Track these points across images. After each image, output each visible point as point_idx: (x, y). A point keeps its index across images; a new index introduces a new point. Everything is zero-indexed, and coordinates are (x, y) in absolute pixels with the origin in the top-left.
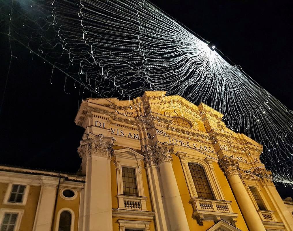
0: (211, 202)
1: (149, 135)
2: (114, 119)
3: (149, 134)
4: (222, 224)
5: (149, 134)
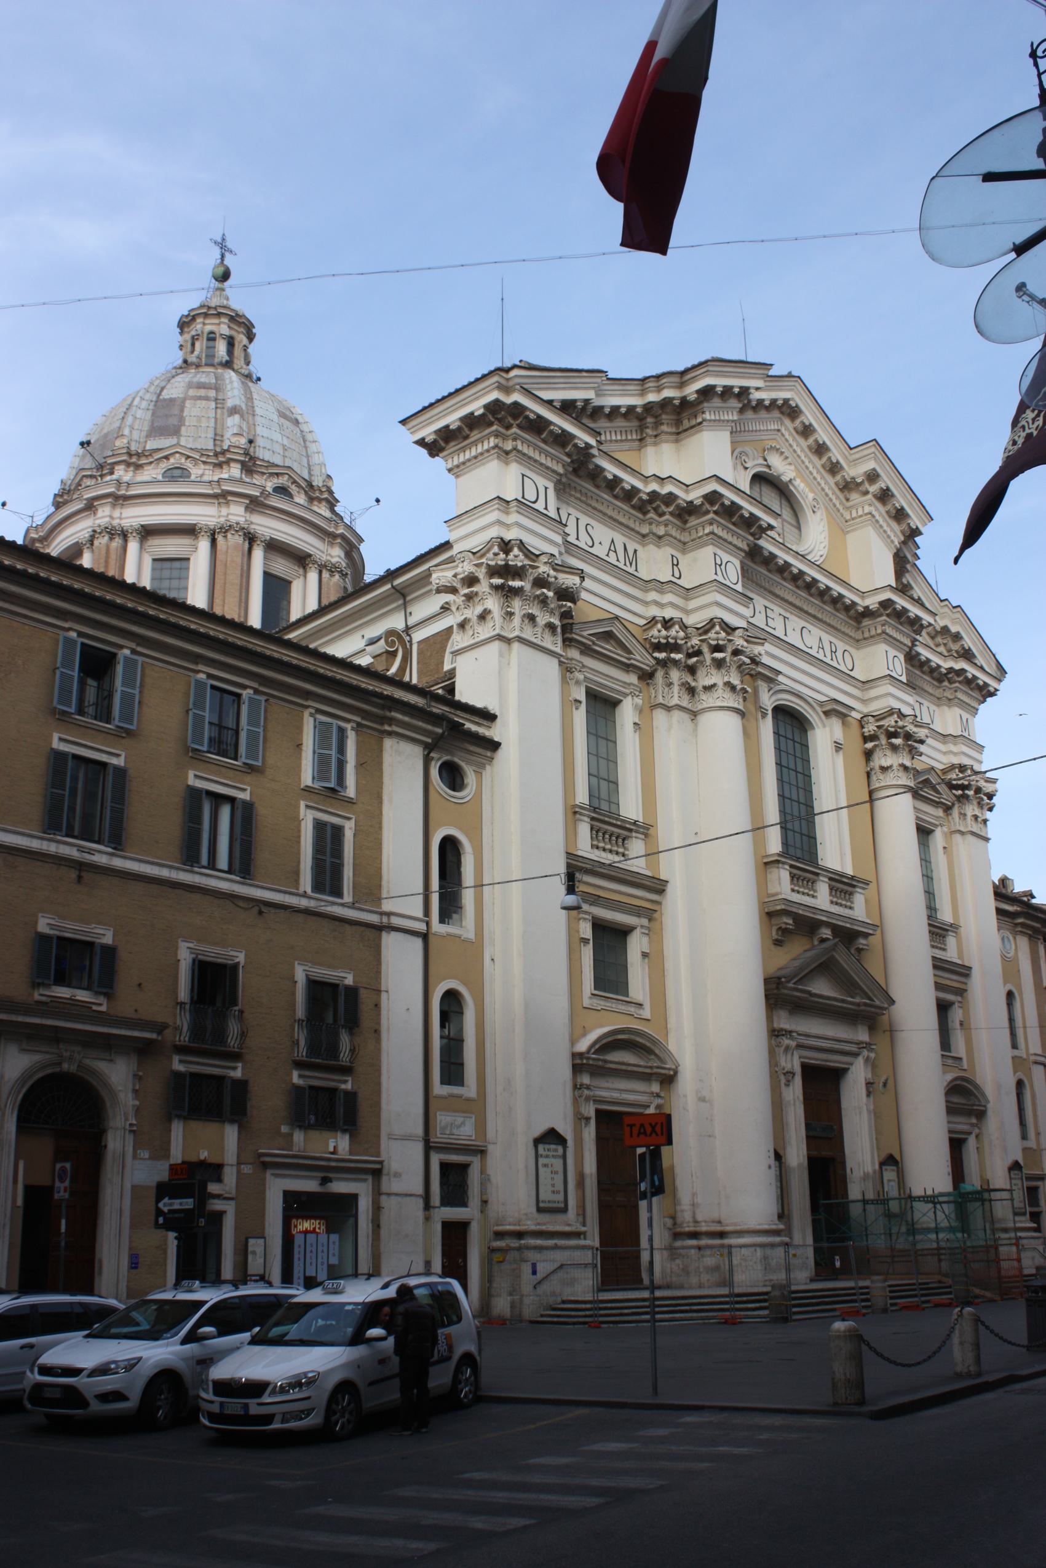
1: (677, 565)
3: (675, 563)
5: (675, 563)
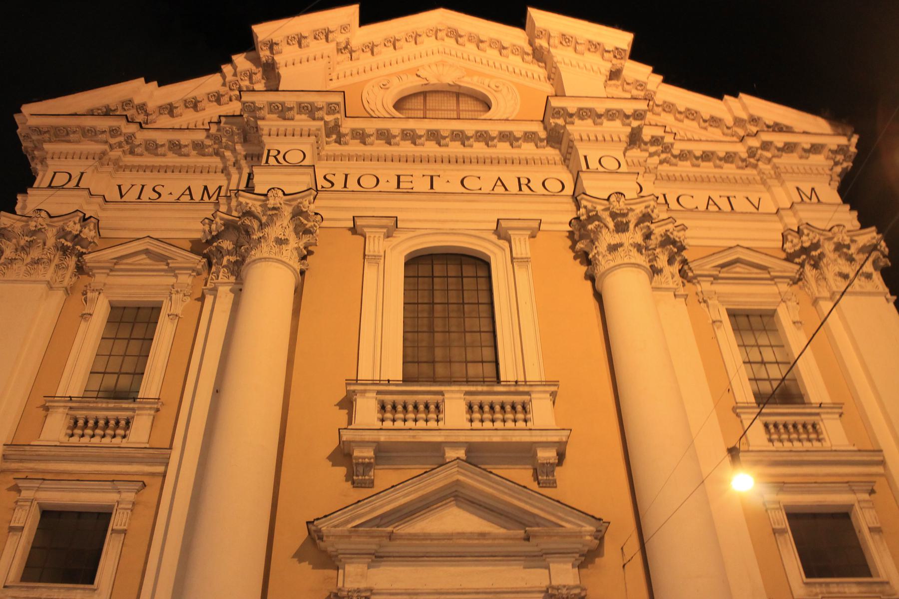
0: (441, 393)
2: (132, 152)
4: (461, 478)
